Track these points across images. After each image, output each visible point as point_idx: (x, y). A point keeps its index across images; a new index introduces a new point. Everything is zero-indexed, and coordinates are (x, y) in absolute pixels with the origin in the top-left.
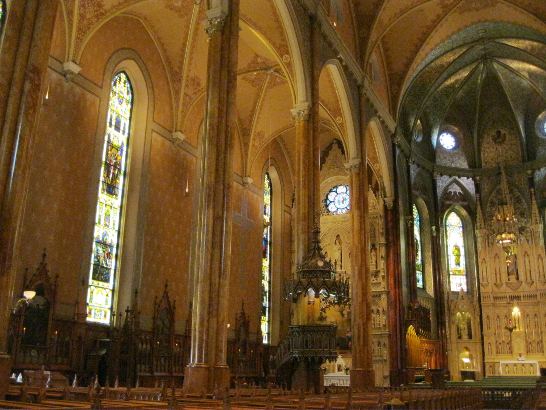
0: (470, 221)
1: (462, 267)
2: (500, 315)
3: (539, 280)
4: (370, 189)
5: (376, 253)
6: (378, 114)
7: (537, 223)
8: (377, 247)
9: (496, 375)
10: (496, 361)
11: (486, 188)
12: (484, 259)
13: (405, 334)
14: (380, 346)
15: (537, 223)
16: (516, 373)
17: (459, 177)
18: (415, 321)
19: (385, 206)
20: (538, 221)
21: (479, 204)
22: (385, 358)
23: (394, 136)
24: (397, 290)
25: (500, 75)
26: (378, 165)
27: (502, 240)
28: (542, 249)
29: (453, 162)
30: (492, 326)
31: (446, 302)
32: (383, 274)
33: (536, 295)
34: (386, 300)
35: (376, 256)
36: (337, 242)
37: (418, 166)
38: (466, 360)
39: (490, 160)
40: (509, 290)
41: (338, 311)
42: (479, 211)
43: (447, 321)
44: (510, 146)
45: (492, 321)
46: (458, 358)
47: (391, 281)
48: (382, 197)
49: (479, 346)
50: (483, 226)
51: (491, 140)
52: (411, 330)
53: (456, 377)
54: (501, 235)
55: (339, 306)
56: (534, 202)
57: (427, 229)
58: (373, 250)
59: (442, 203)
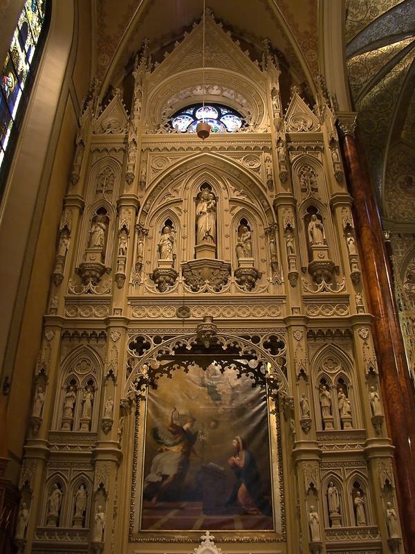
55: (205, 369)
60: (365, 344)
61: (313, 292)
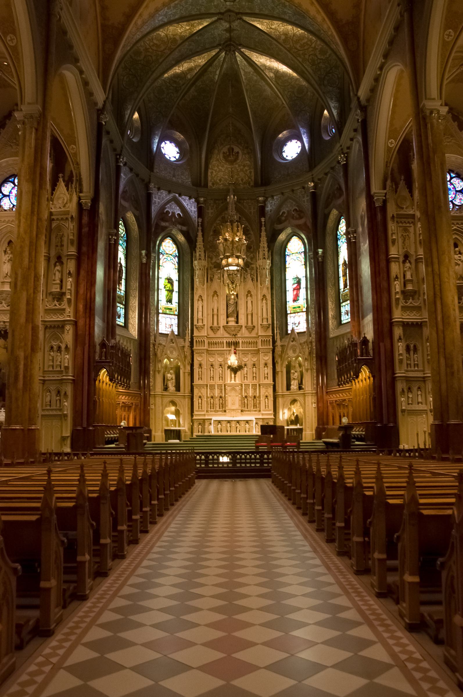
0: (188, 250)
1: (175, 305)
2: (214, 363)
3: (261, 325)
4: (61, 180)
5: (62, 268)
6: (79, 64)
7: (264, 258)
8: (64, 260)
9: (206, 434)
10: (206, 417)
11: (210, 212)
12: (201, 296)
13: (95, 380)
14: (60, 396)
15: (264, 258)
16: (229, 432)
17: (180, 195)
18: (109, 362)
19: (80, 205)
20: (266, 257)
21: (200, 231)
22: (65, 413)
23: (100, 112)
24: (88, 320)
25: (242, 73)
26: (74, 147)
27: (228, 265)
28: (268, 288)
29: (174, 176)
30: (204, 377)
31: (151, 346)
32: (69, 297)
33: (257, 342)
34: (71, 332)
35: (62, 272)
36: (8, 249)
37: (131, 170)
38: (172, 417)
39: (218, 181)
40: (227, 335)
41: (3, 347)
42: (200, 239)
43: (151, 368)
44: (242, 167)
45: (204, 371)
46: (163, 413)
47: (81, 307)
48: (76, 192)
49: (187, 401)
50: (203, 258)
51: (221, 157)
52: (103, 374)
53: (158, 437)
54: (228, 259)
55: (5, 341)
56: (263, 234)
57: (135, 251)
58: (57, 264)
59: (157, 225)
60: (68, 333)
61: (49, 307)
